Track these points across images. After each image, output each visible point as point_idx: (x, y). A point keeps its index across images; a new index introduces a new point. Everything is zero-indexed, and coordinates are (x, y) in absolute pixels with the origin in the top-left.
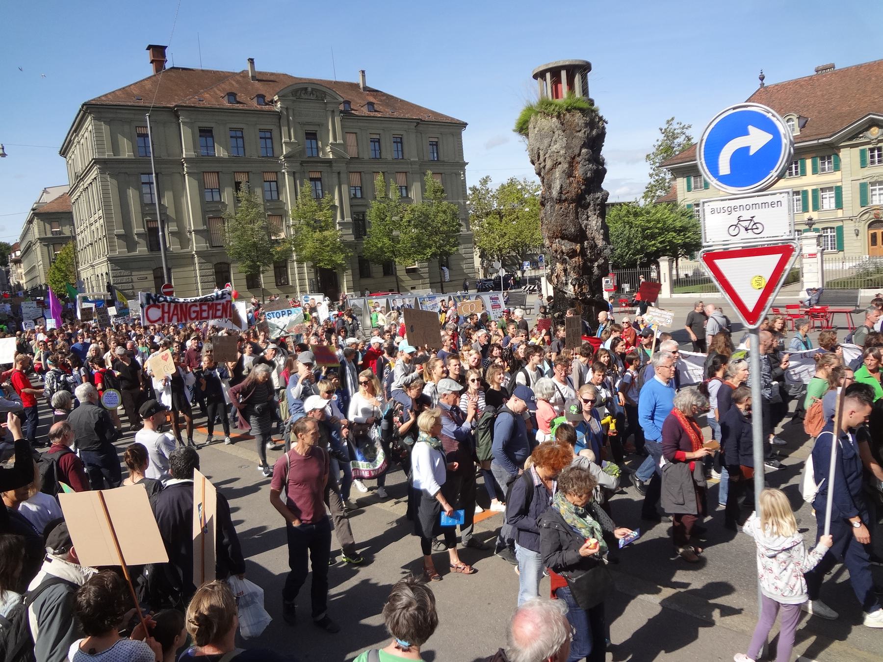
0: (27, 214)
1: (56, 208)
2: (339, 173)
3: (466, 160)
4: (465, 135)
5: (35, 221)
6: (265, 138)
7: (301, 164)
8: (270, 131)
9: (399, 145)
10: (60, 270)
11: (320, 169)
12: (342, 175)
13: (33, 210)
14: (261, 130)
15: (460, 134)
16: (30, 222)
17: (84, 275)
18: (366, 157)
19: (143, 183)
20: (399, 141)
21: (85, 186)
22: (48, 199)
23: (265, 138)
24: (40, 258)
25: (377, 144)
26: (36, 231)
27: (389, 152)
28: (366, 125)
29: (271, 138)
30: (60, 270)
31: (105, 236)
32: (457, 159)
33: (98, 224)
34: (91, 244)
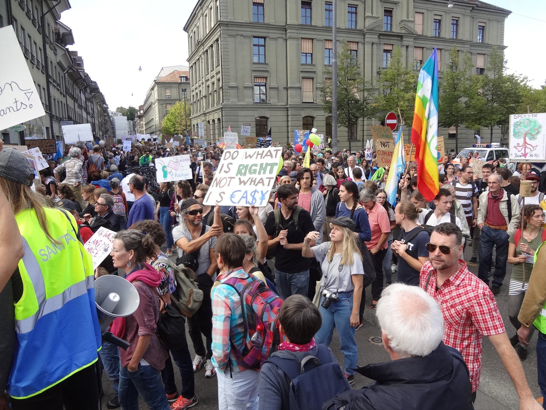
0: (151, 83)
1: (169, 80)
2: (407, 47)
3: (505, 44)
4: (508, 21)
5: (156, 88)
6: (352, 13)
7: (379, 36)
8: (356, 7)
9: (455, 26)
10: (170, 121)
11: (392, 42)
12: (409, 49)
13: (155, 81)
14: (350, 6)
15: (504, 21)
16: (152, 89)
17: (194, 122)
18: (429, 35)
19: (254, 45)
20: (456, 23)
21: (205, 49)
22: (164, 74)
23: (352, 13)
24: (157, 112)
25: (438, 24)
26: (155, 95)
27: (447, 32)
28: (433, 6)
29: (356, 13)
30: (170, 121)
31: (222, 88)
32: (499, 43)
33: (201, 88)
34: (205, 97)
